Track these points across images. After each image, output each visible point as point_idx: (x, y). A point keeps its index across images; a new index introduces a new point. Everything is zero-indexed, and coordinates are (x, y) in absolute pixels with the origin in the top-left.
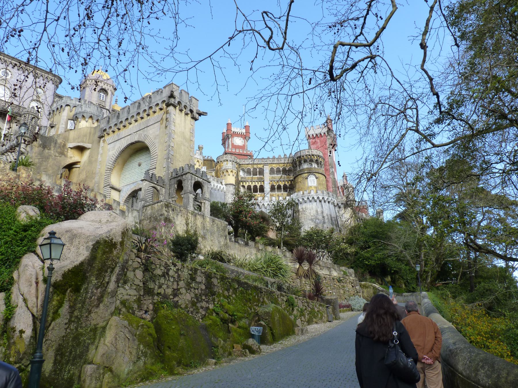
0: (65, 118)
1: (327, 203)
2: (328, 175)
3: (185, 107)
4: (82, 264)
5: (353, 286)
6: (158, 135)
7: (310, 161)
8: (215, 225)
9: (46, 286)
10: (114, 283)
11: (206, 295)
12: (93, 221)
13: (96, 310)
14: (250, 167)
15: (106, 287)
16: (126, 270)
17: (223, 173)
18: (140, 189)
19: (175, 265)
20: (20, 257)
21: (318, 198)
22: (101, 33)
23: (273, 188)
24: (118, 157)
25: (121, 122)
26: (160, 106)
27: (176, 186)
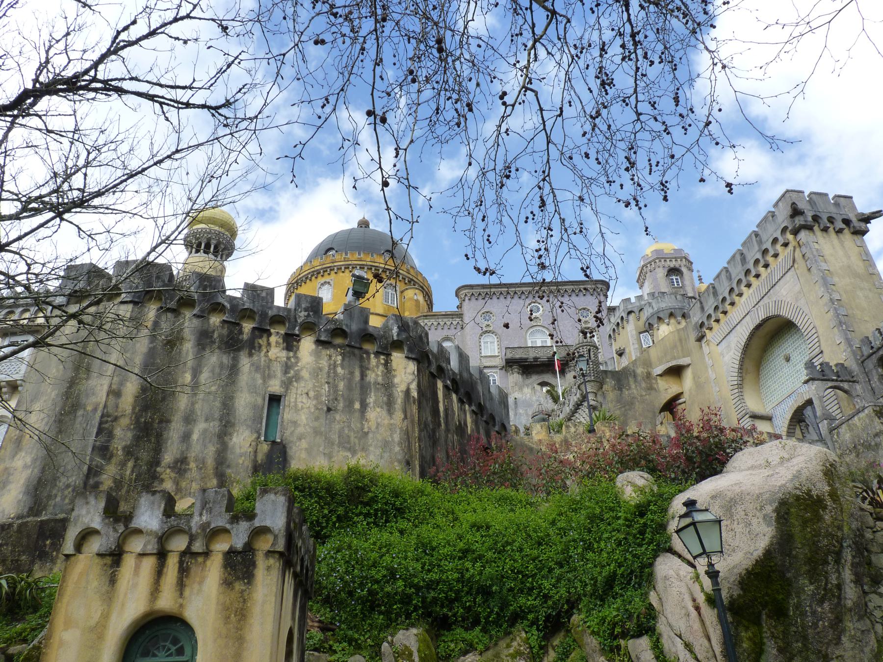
0: (634, 332)
3: (831, 220)
6: (799, 292)
9: (716, 610)
10: (852, 585)
12: (753, 467)
13: (838, 653)
15: (839, 598)
16: (866, 554)
18: (809, 402)
20: (651, 565)
22: (637, 101)
25: (724, 299)
26: (781, 240)
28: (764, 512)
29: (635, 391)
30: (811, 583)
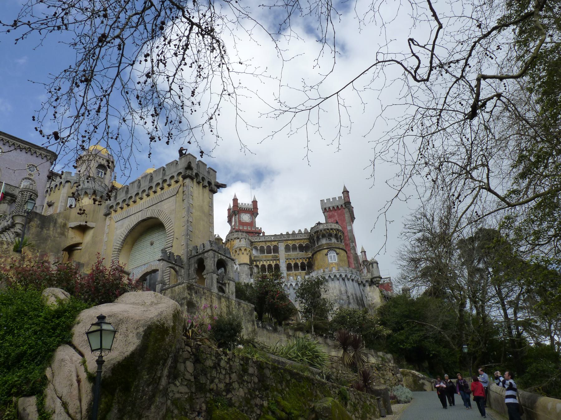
0: (65, 195)
1: (351, 281)
2: (349, 250)
3: (203, 179)
4: (133, 354)
5: (393, 374)
6: (173, 210)
7: (329, 235)
8: (241, 309)
9: (92, 384)
10: (166, 378)
11: (259, 390)
12: (133, 303)
13: (147, 414)
14: (263, 244)
15: (158, 384)
17: (236, 251)
18: (155, 271)
19: (226, 355)
20: (54, 350)
21: (341, 276)
22: (173, 81)
23: (289, 267)
24: (127, 236)
25: (131, 197)
26: (176, 179)
27: (196, 265)
28: (138, 331)
29: (51, 233)
30: (148, 374)
